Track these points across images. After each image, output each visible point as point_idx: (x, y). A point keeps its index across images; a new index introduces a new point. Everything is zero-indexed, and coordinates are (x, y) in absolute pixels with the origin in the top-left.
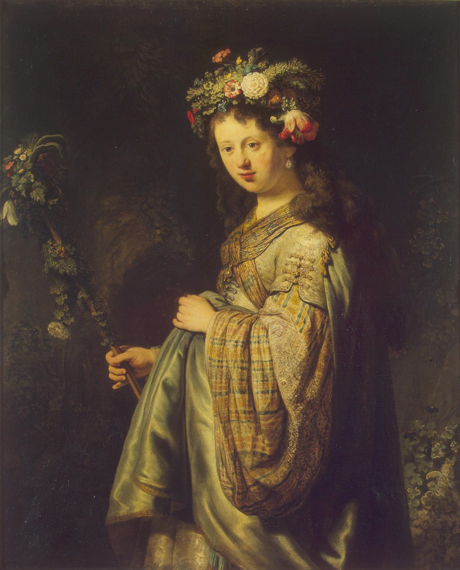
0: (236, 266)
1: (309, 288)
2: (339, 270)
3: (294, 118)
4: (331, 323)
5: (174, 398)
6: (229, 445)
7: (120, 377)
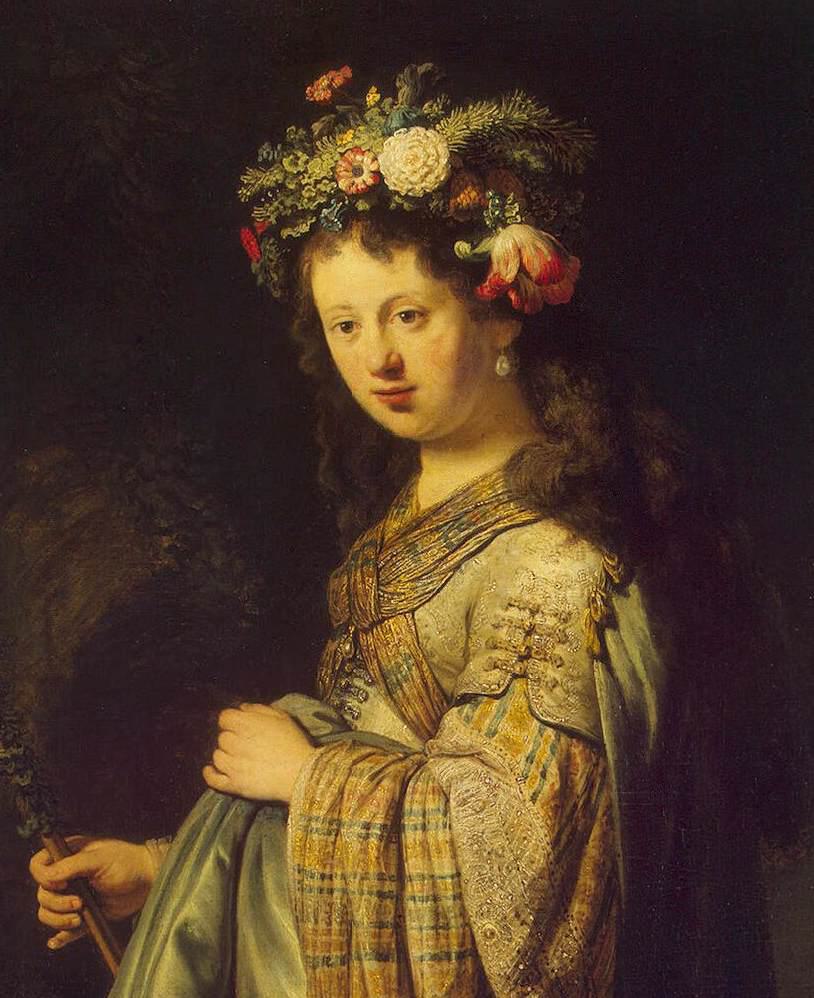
0: (366, 631)
1: (554, 686)
4: (613, 776)
5: (207, 973)
7: (66, 918)
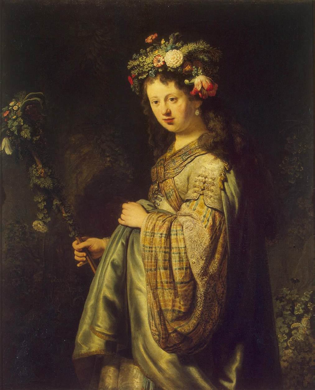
0: (161, 183)
1: (211, 197)
3: (201, 80)
4: (226, 221)
5: (119, 273)
7: (82, 258)
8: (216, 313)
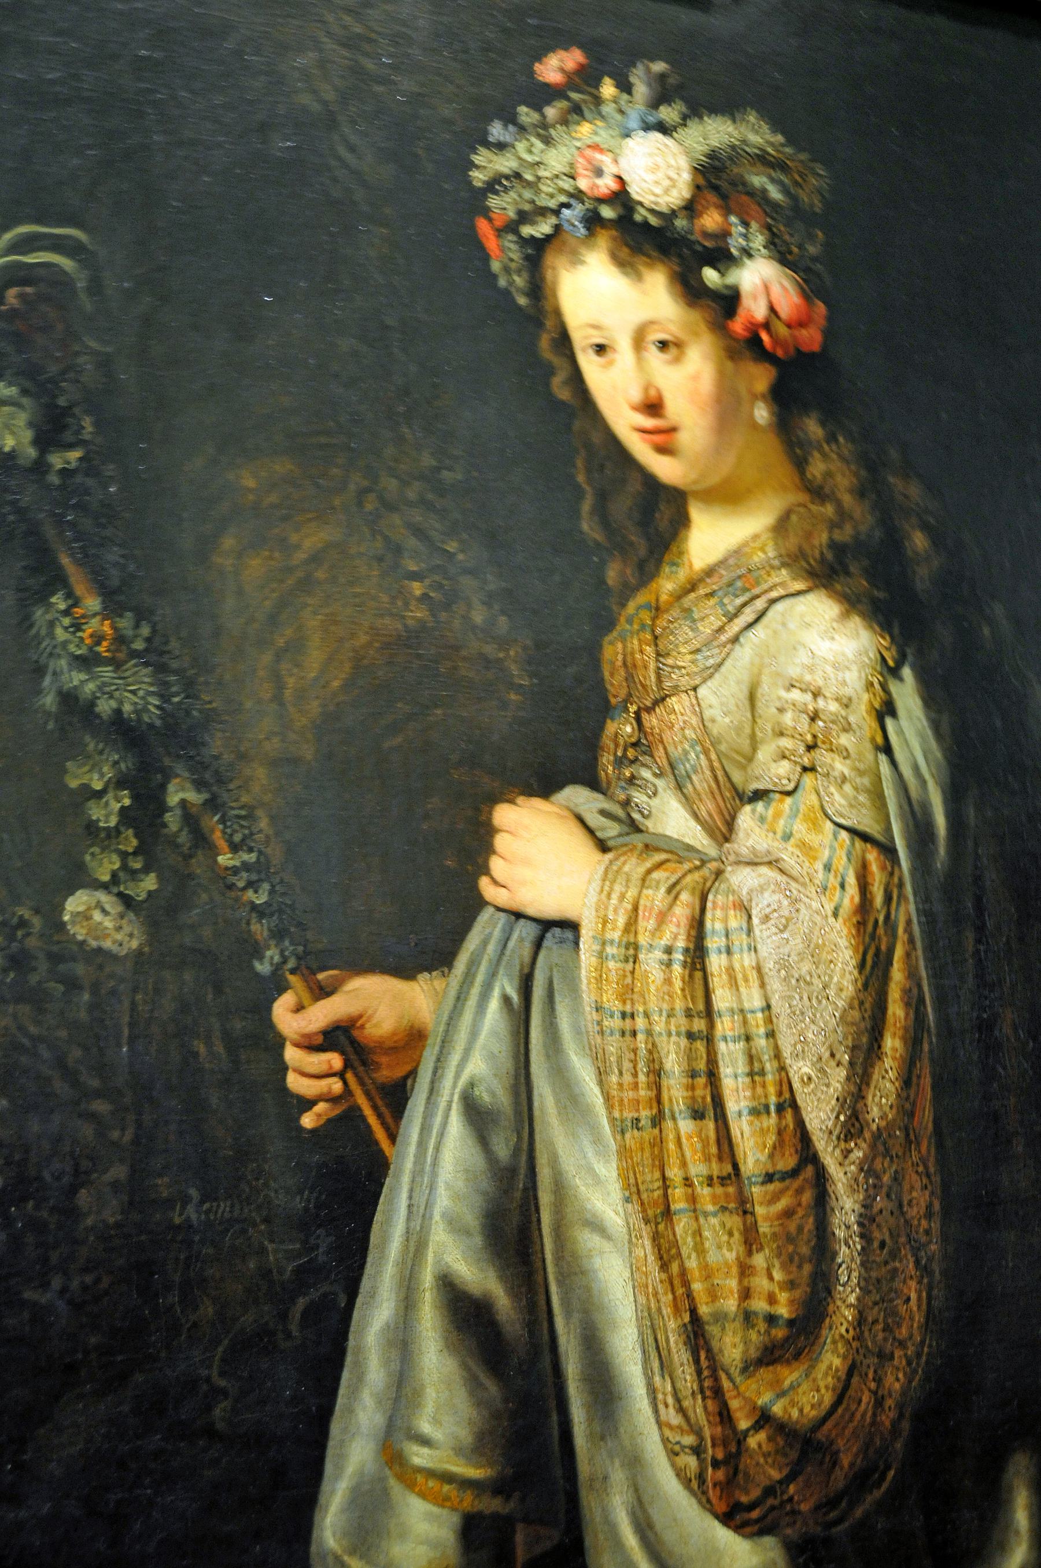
0: (649, 710)
2: (912, 728)
4: (909, 889)
5: (502, 1150)
6: (675, 1298)
8: (915, 1309)
